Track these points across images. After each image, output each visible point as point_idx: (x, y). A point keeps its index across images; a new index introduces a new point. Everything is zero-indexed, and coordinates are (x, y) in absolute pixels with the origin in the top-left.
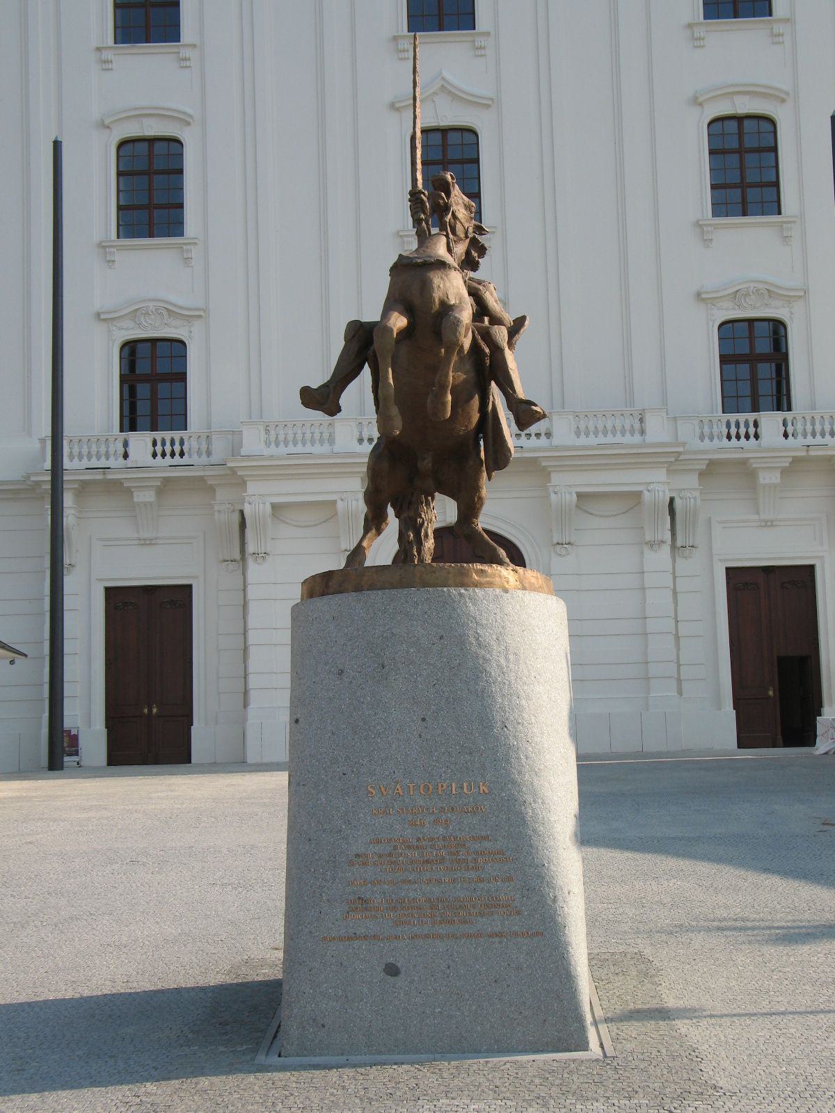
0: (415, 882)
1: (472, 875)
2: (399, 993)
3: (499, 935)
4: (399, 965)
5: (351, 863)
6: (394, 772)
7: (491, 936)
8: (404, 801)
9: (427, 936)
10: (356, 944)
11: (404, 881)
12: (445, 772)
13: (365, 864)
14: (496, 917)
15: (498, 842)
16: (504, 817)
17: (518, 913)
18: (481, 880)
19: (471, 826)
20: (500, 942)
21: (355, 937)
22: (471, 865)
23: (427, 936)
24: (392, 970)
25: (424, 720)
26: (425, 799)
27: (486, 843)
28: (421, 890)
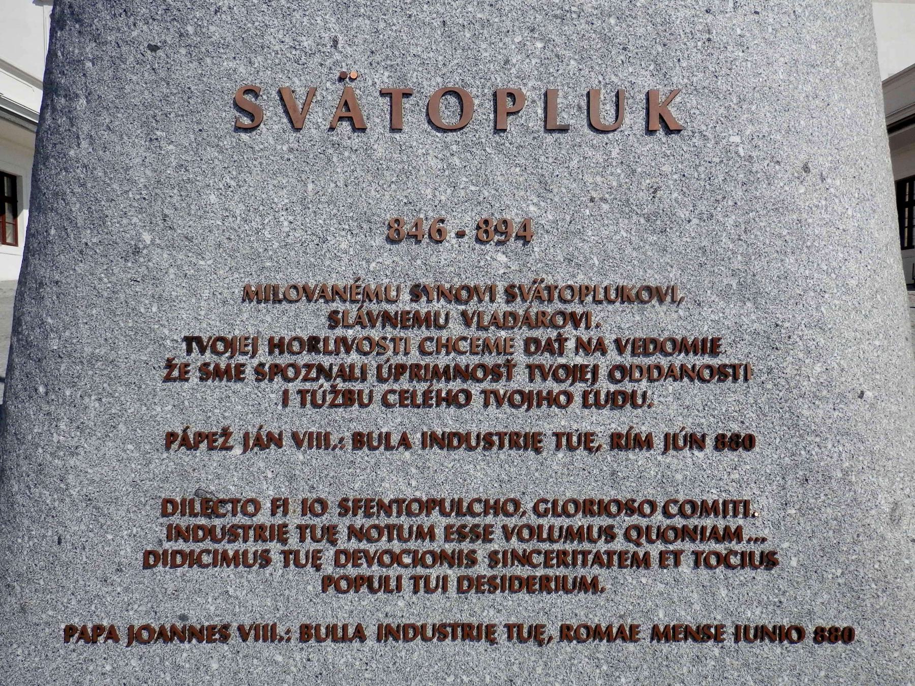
0: (405, 442)
3: (702, 634)
5: (175, 372)
6: (335, 42)
7: (660, 634)
8: (368, 150)
9: (441, 631)
10: (188, 650)
11: (359, 441)
12: (522, 45)
15: (706, 311)
16: (730, 221)
17: (769, 561)
18: (646, 443)
19: (610, 246)
22: (605, 386)
23: (441, 631)
26: (447, 146)
27: (661, 309)
28: (422, 469)
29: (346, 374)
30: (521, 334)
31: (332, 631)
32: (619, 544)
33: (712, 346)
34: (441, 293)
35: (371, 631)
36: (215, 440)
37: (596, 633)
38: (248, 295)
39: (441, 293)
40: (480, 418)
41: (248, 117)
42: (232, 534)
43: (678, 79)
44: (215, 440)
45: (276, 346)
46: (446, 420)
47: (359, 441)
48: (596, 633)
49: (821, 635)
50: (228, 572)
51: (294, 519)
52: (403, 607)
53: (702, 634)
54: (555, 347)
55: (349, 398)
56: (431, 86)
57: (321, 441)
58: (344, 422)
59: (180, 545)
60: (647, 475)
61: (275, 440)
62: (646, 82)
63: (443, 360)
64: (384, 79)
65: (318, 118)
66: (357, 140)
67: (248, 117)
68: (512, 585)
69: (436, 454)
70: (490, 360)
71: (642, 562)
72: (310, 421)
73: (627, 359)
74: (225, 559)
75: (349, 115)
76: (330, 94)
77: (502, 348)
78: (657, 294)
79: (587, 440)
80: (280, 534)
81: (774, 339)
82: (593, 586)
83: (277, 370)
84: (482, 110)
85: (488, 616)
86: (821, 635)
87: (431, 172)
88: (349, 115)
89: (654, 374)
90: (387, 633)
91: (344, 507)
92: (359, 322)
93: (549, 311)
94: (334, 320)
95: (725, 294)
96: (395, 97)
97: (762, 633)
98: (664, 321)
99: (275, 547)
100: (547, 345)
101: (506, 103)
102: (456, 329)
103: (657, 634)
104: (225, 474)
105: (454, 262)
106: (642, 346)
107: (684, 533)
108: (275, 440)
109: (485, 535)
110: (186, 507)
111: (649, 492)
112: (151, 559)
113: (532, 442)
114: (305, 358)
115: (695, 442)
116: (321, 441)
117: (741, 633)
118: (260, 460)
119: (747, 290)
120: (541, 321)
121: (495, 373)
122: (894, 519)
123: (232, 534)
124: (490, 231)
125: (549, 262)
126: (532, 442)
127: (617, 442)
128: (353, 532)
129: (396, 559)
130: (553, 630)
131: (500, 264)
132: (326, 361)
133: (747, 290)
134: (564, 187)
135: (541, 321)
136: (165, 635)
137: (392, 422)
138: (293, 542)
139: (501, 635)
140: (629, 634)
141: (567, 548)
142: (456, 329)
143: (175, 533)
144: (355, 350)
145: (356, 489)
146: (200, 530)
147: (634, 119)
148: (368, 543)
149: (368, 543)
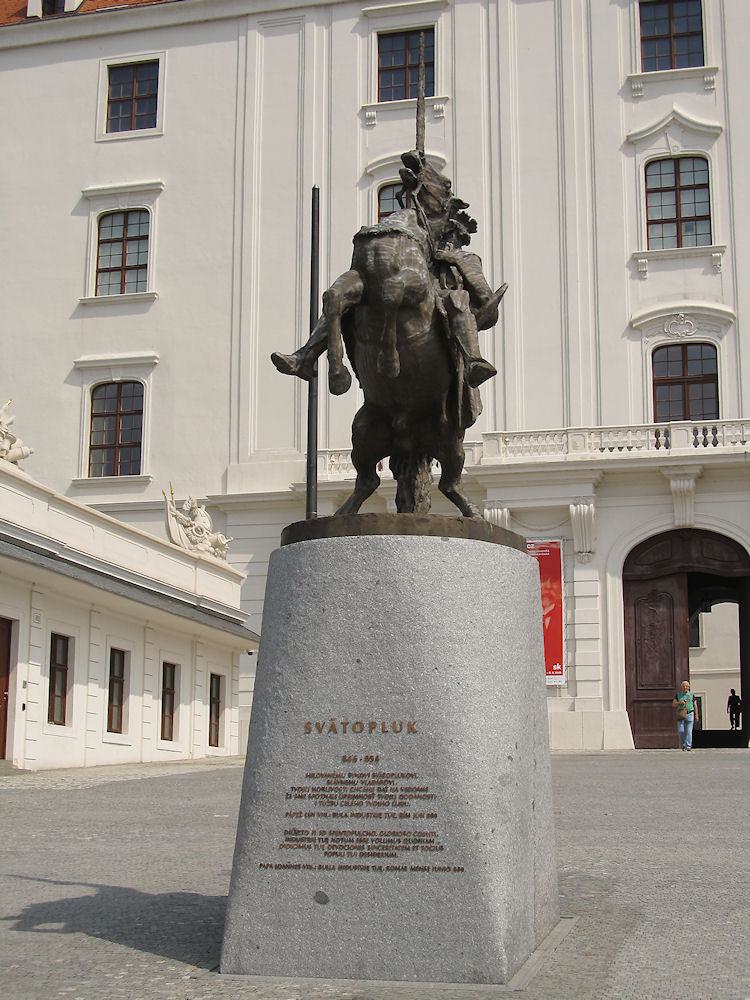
1: (398, 811)
2: (327, 921)
3: (423, 869)
4: (327, 893)
5: (288, 796)
9: (355, 868)
11: (335, 815)
13: (301, 797)
14: (419, 851)
20: (423, 876)
21: (289, 867)
22: (398, 801)
23: (355, 868)
24: (322, 899)
25: (358, 661)
29: (331, 797)
30: (376, 787)
31: (327, 867)
32: (401, 844)
33: (426, 789)
34: (356, 775)
35: (337, 867)
36: (299, 815)
37: (396, 869)
38: (307, 776)
39: (356, 775)
40: (366, 809)
41: (308, 730)
42: (302, 840)
43: (416, 719)
44: (299, 815)
45: (314, 789)
46: (357, 810)
47: (335, 815)
48: (396, 869)
49: (455, 869)
50: (301, 850)
51: (318, 837)
52: (345, 861)
53: (423, 869)
54: (385, 790)
55: (333, 803)
56: (354, 721)
57: (325, 815)
58: (333, 810)
59: (286, 843)
60: (409, 825)
61: (313, 815)
62: (408, 719)
63: (356, 793)
64: (342, 720)
65: (325, 730)
66: (335, 735)
67: (308, 730)
68: (374, 855)
69: (354, 819)
70: (368, 793)
71: (408, 849)
72: (322, 810)
73: (403, 793)
74: (300, 847)
75: (333, 729)
76: (328, 724)
77: (371, 790)
78: (411, 775)
79: (393, 815)
80: (314, 840)
81: (441, 788)
82: (394, 855)
83: (314, 796)
84: (367, 728)
85: (368, 864)
86: (455, 869)
87: (353, 744)
88: (333, 729)
89: (411, 797)
90: (340, 868)
91: (331, 833)
92: (335, 783)
93: (383, 780)
94: (329, 783)
95: (430, 775)
96: (345, 724)
97: (440, 869)
98: (414, 783)
99: (312, 844)
100: (380, 788)
101: (373, 726)
102: (359, 785)
103: (412, 869)
104: (300, 824)
105: (359, 767)
106: (407, 790)
107: (419, 841)
108: (313, 815)
109: (366, 841)
110: (290, 833)
111: (410, 829)
112: (282, 846)
113: (379, 815)
114: (322, 793)
115: (422, 816)
116: (325, 815)
117: (434, 869)
118: (310, 821)
119: (435, 774)
120: (381, 782)
121: (370, 797)
122: (477, 838)
123: (302, 840)
124: (368, 759)
125: (383, 767)
126: (379, 815)
127: (402, 816)
128: (333, 840)
129: (344, 848)
130: (384, 867)
131: (371, 767)
132: (326, 794)
133: (435, 774)
134: (387, 747)
135: (381, 782)
136: (284, 867)
137: (343, 810)
138: (317, 843)
139: (371, 869)
140: (405, 869)
141: (385, 846)
142: (359, 785)
143: (287, 839)
144: (333, 790)
145: (334, 828)
146: (294, 838)
147: (405, 729)
148: (337, 843)
149: (337, 843)
